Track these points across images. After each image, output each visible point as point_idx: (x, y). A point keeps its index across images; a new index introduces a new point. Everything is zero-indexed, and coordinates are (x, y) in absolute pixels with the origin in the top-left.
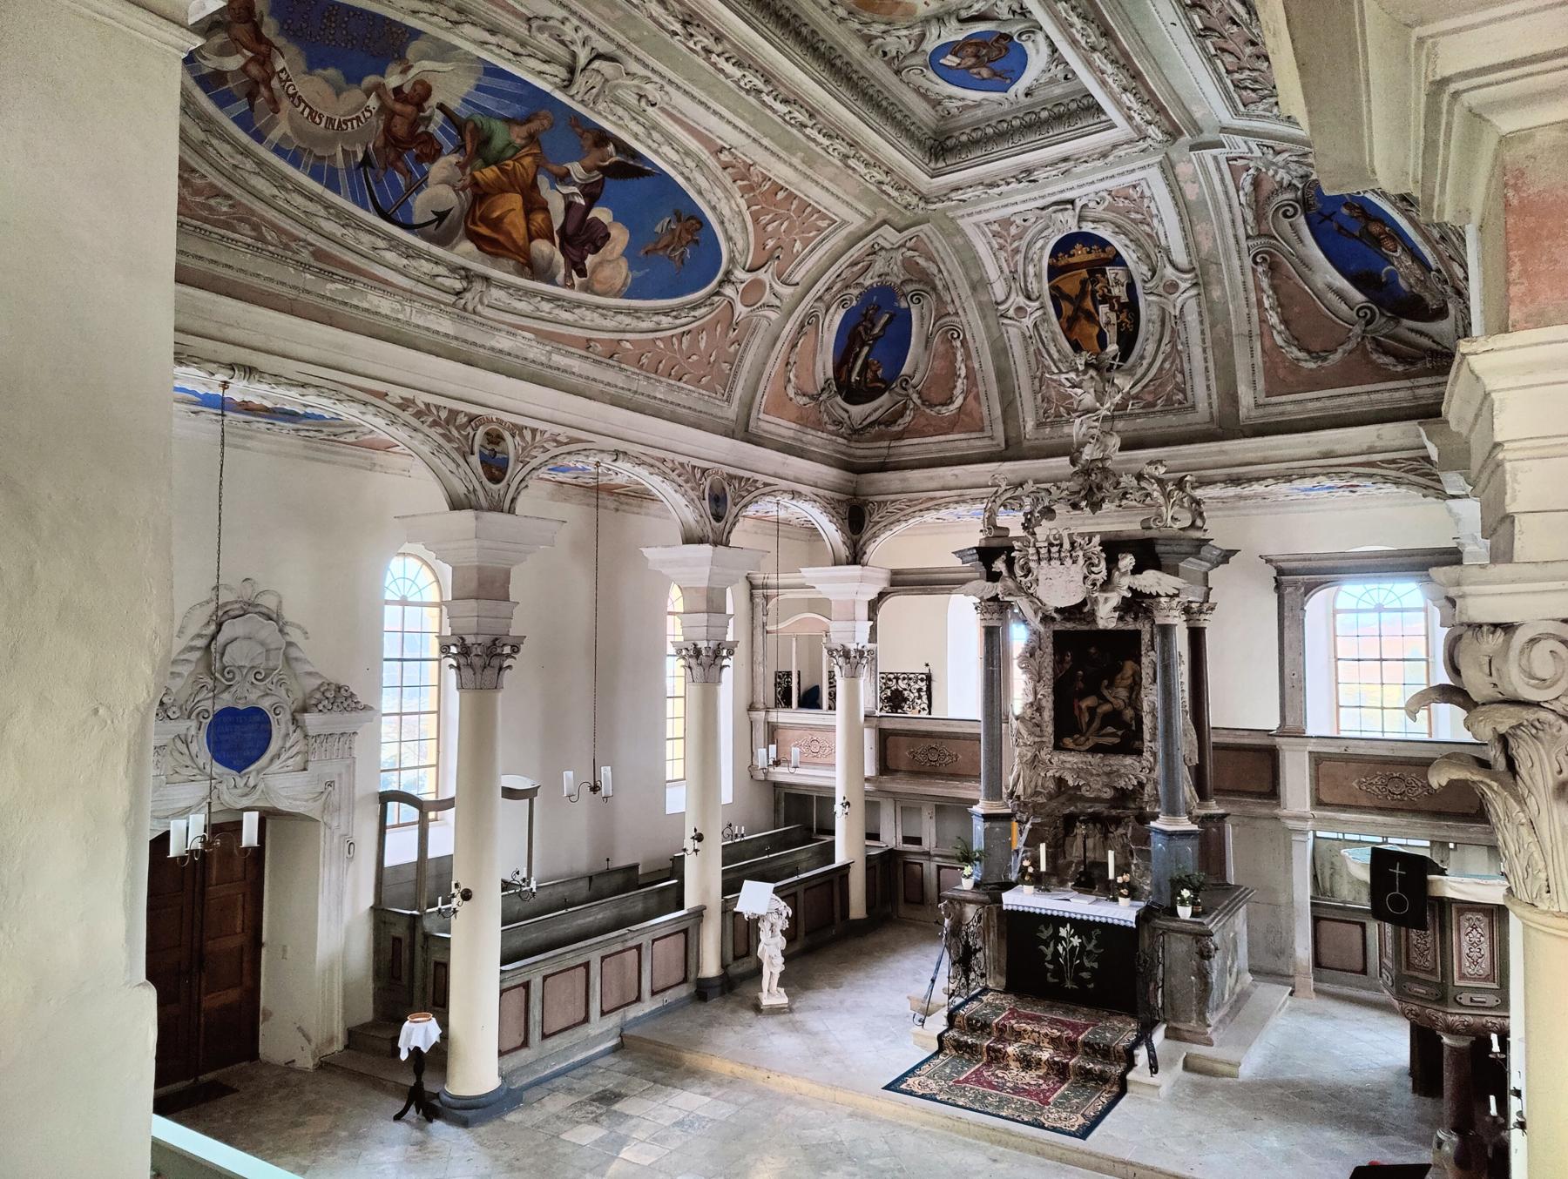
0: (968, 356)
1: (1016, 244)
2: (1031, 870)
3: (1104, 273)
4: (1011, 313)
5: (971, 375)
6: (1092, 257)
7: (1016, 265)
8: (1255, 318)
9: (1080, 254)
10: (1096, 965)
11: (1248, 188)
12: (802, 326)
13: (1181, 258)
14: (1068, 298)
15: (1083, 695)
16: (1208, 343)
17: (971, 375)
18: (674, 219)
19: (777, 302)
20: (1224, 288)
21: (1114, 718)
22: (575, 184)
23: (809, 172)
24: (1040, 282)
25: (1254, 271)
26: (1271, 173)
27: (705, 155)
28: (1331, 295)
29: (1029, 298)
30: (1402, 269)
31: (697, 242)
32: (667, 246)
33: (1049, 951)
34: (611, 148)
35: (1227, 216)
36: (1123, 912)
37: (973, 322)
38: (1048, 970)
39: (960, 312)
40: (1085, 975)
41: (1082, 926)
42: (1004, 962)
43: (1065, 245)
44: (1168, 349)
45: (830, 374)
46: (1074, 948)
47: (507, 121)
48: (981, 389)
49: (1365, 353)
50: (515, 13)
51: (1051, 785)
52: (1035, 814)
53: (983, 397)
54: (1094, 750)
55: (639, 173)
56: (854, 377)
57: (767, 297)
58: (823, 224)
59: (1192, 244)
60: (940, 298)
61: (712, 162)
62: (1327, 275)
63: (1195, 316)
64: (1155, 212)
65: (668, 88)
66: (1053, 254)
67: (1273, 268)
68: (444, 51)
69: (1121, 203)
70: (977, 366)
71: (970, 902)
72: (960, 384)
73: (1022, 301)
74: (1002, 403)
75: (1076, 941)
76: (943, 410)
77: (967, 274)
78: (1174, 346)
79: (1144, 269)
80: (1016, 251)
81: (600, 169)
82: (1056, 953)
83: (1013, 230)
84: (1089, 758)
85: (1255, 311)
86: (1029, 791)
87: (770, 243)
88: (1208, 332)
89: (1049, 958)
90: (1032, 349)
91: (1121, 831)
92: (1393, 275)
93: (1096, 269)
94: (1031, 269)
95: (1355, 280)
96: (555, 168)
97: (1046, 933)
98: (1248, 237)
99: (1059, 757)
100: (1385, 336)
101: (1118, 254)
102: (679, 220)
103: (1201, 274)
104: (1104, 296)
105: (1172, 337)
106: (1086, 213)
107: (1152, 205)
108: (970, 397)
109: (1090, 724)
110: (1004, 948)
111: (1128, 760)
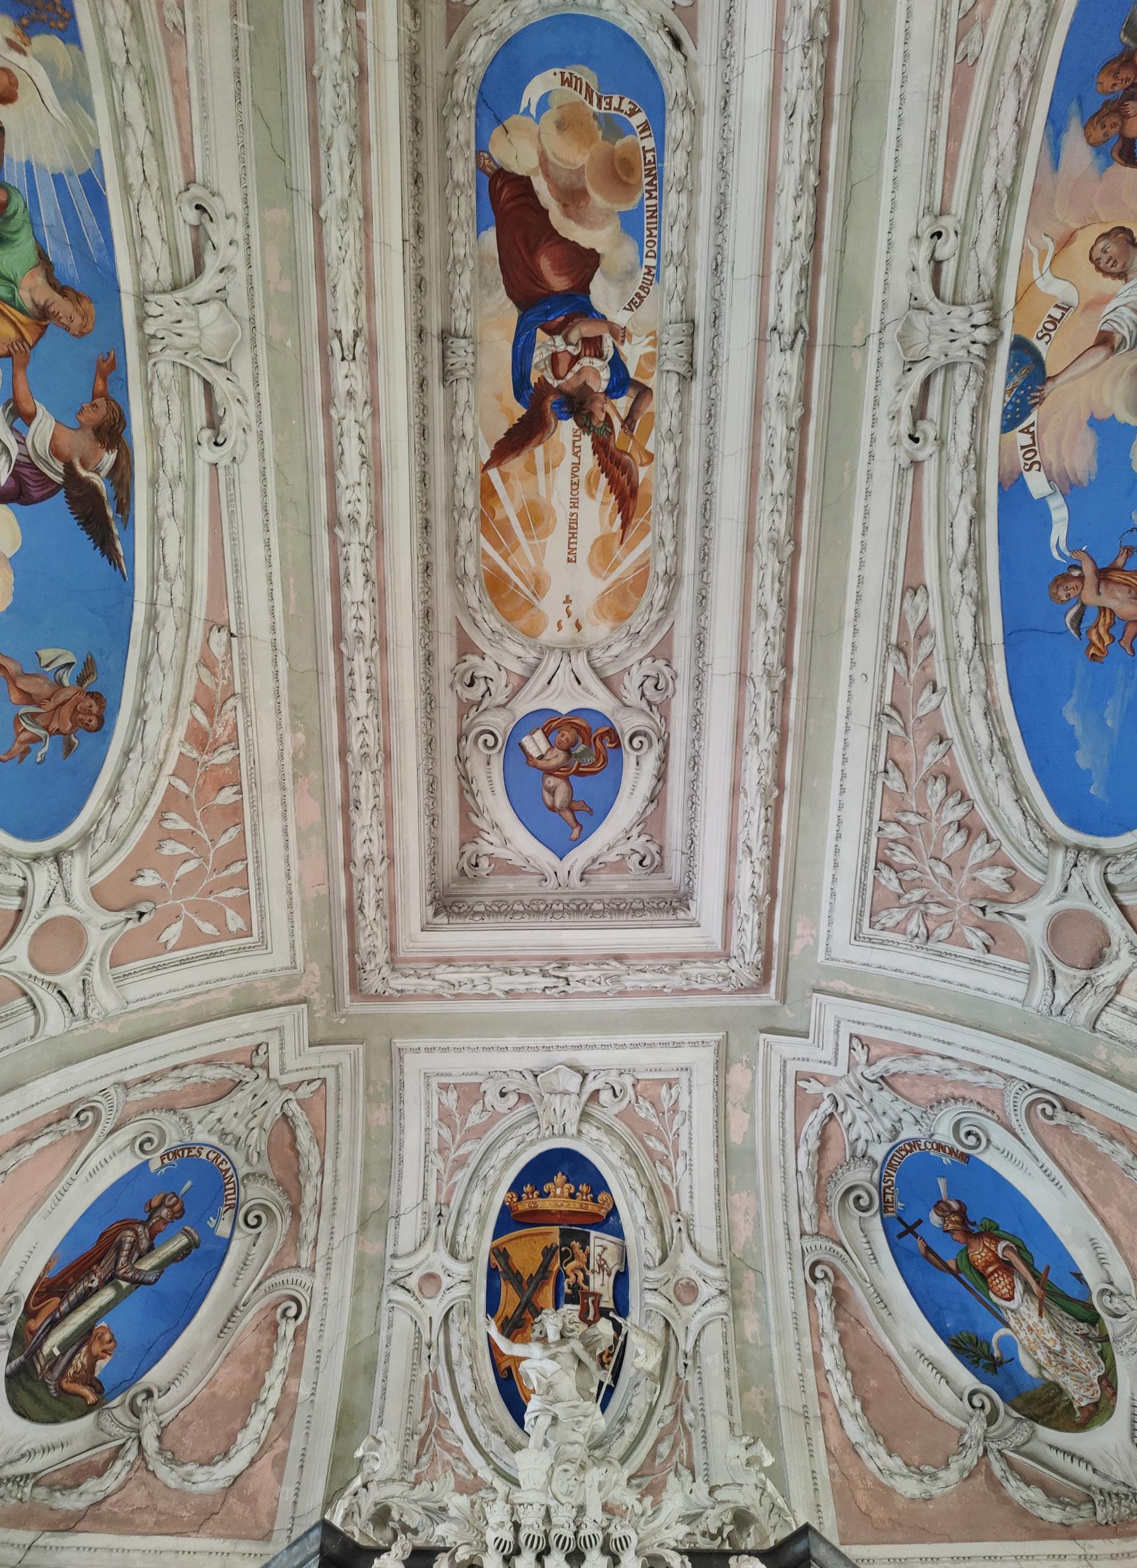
0: (295, 1368)
1: (462, 1151)
3: (585, 1241)
4: (412, 1282)
5: (288, 1400)
6: (574, 1206)
7: (451, 1192)
8: (812, 1389)
9: (559, 1196)
11: (814, 1144)
12: (63, 1115)
13: (706, 1236)
14: (515, 1278)
16: (737, 1419)
17: (288, 1400)
18: (77, 670)
19: (77, 1001)
20: (764, 1322)
22: (21, 442)
23: (289, 784)
24: (480, 1232)
25: (811, 1294)
26: (847, 1118)
27: (200, 610)
28: (923, 1367)
29: (454, 1254)
30: (1028, 1331)
31: (69, 747)
32: (29, 698)
34: (109, 459)
35: (778, 1188)
37: (331, 1293)
39: (320, 1267)
43: (539, 1171)
44: (669, 1414)
45: (26, 1287)
47: (42, 255)
48: (297, 1443)
49: (995, 1484)
50: (187, 158)
53: (292, 1463)
55: (104, 540)
56: (52, 1345)
57: (69, 980)
58: (235, 922)
59: (724, 1222)
60: (295, 1237)
61: (198, 629)
62: (911, 1334)
63: (718, 1358)
64: (683, 1146)
65: (252, 438)
66: (516, 1187)
67: (839, 1297)
68: (74, 93)
69: (645, 1111)
70: (304, 1392)
72: (260, 1421)
73: (438, 1259)
74: (330, 1482)
76: (200, 1474)
77: (364, 1191)
78: (679, 1412)
79: (652, 1244)
80: (461, 1163)
81: (69, 467)
83: (475, 1117)
85: (810, 1372)
87: (150, 879)
88: (735, 1393)
90: (424, 1371)
92: (1008, 1344)
93: (576, 1229)
94: (476, 1199)
95: (958, 1347)
96: (22, 389)
98: (803, 1234)
100: (1016, 1450)
101: (614, 1211)
102: (81, 680)
103: (738, 1278)
104: (575, 1287)
105: (676, 1395)
106: (594, 1110)
107: (684, 1132)
108: (267, 1460)
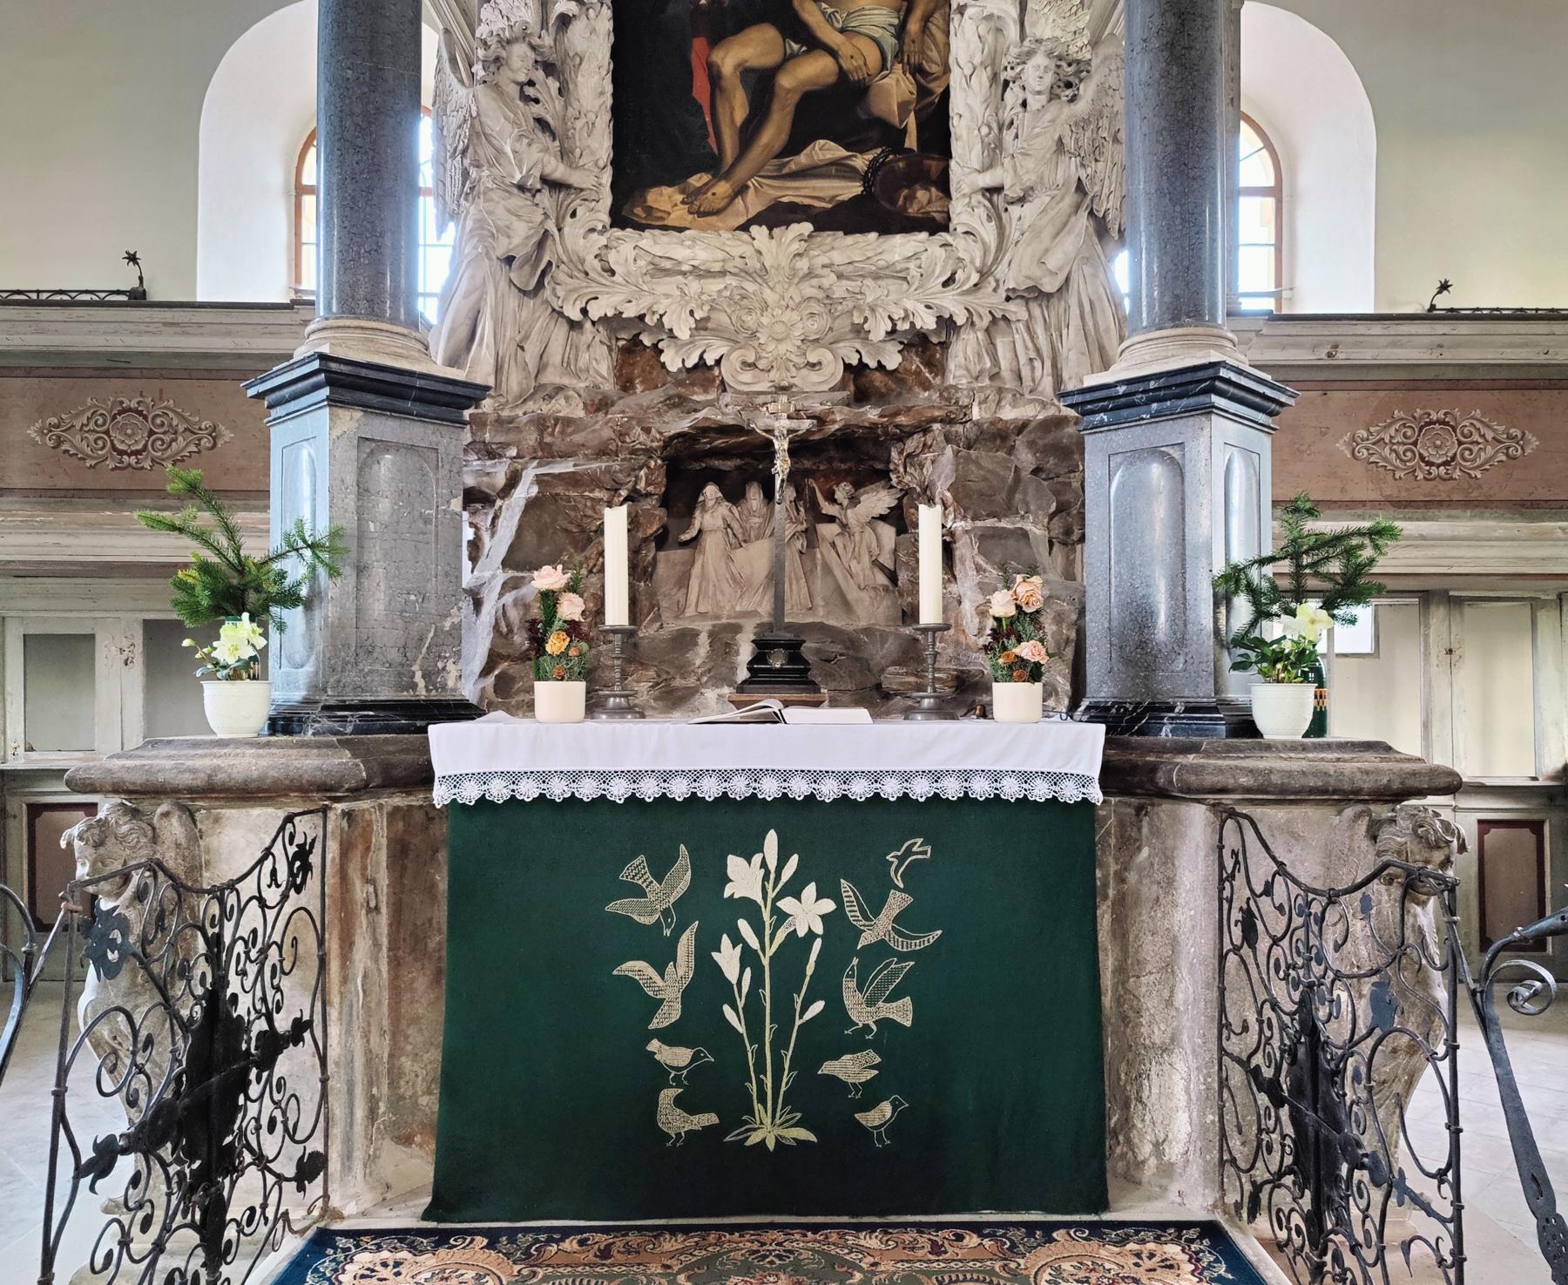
2: (571, 608)
10: (902, 1012)
15: (723, 28)
21: (838, 109)
33: (668, 986)
36: (1032, 745)
38: (659, 1075)
40: (851, 1068)
41: (835, 833)
42: (422, 1068)
46: (797, 945)
51: (599, 363)
52: (546, 453)
54: (777, 216)
71: (247, 793)
75: (808, 912)
82: (708, 985)
84: (759, 231)
86: (514, 381)
89: (669, 1014)
91: (878, 500)
97: (654, 897)
99: (629, 247)
109: (749, 133)
110: (427, 1006)
111: (901, 246)
